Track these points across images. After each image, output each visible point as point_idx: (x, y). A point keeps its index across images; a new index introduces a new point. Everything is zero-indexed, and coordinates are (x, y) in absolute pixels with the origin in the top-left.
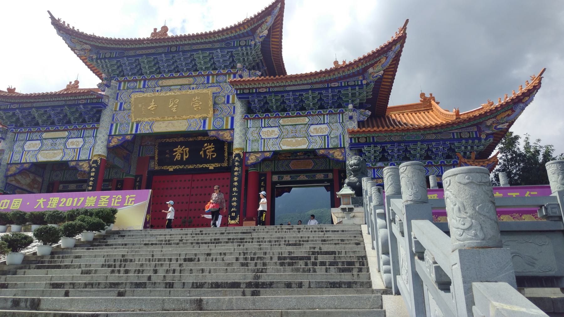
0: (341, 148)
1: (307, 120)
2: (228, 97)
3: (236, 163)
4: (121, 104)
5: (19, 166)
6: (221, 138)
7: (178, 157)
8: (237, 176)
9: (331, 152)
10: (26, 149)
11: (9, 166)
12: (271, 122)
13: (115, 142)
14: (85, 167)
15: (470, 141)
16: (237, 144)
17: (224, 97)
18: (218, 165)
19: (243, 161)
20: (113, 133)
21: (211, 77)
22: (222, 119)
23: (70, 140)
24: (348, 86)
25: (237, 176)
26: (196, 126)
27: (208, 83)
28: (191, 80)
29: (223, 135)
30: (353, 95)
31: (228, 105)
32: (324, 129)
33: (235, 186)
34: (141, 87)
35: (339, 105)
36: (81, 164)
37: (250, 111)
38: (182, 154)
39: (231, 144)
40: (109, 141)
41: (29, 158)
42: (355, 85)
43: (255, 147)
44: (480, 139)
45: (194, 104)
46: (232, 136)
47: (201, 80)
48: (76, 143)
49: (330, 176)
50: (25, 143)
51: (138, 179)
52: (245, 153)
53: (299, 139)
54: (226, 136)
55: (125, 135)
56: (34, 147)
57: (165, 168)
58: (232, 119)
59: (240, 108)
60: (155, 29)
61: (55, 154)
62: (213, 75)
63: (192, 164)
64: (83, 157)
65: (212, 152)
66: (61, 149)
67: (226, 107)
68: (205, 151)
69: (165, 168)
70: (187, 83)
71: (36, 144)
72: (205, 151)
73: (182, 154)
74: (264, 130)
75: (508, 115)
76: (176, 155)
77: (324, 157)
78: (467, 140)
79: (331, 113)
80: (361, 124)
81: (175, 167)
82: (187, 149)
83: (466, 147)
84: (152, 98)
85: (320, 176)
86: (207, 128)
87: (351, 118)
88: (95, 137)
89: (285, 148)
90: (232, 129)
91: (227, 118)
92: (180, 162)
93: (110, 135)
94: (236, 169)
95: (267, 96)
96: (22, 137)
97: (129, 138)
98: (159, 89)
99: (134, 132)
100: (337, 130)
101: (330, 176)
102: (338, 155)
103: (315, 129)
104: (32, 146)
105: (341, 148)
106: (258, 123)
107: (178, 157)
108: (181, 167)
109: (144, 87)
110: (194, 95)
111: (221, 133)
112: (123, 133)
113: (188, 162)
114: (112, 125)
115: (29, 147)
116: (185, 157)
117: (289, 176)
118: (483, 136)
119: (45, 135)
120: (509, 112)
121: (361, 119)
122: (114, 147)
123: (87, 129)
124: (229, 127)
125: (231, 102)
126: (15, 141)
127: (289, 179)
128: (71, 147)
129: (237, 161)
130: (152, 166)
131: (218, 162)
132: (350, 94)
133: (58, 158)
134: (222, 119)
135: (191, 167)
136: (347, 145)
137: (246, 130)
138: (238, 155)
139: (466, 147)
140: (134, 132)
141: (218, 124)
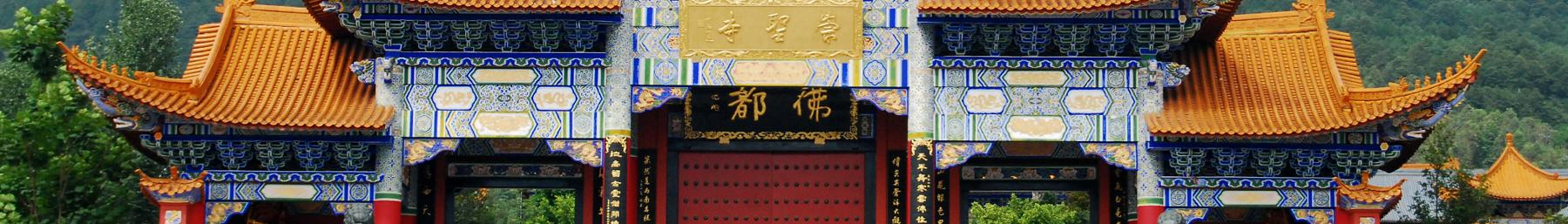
0: (1129, 142)
1: (1060, 78)
2: (893, 12)
3: (921, 167)
4: (650, 11)
5: (430, 145)
6: (881, 106)
7: (741, 112)
8: (924, 193)
9: (1110, 149)
11: (407, 143)
12: (989, 77)
13: (646, 102)
14: (588, 155)
15: (1362, 153)
17: (884, 10)
18: (835, 136)
19: (931, 160)
20: (642, 81)
23: (541, 91)
24: (1151, 20)
25: (924, 193)
29: (884, 100)
31: (894, 31)
32: (1094, 101)
33: (920, 214)
35: (1130, 52)
36: (576, 146)
37: (940, 50)
38: (750, 107)
39: (904, 119)
41: (455, 129)
42: (1162, 19)
44: (1377, 148)
46: (906, 103)
48: (555, 97)
49: (1092, 172)
51: (647, 160)
52: (935, 143)
53: (1047, 119)
54: (891, 103)
56: (457, 100)
57: (710, 135)
58: (905, 63)
59: (920, 48)
61: (512, 120)
64: (580, 132)
65: (822, 103)
66: (525, 111)
67: (886, 35)
68: (804, 102)
69: (710, 135)
71: (462, 95)
72: (804, 102)
73: (750, 107)
75: (1426, 118)
76: (735, 107)
77: (1096, 160)
78: (1357, 148)
79: (1112, 68)
80: (1170, 95)
81: (739, 135)
82: (764, 95)
83: (1355, 161)
86: (850, 84)
87: (1151, 84)
88: (600, 86)
90: (905, 87)
92: (747, 124)
93: (635, 84)
94: (921, 177)
95: (984, 26)
97: (678, 93)
101: (1092, 172)
102: (1121, 157)
103: (1078, 98)
104: (452, 98)
105: (1129, 142)
106: (958, 77)
107: (741, 112)
111: (881, 95)
112: (666, 81)
113: (767, 123)
114: (636, 62)
118: (1384, 147)
120: (1427, 113)
121: (1171, 84)
122: (647, 113)
123: (580, 67)
125: (898, 24)
126: (409, 85)
127: (1001, 177)
129: (922, 161)
131: (837, 130)
132: (1152, 37)
133: (523, 131)
135: (771, 136)
138: (923, 149)
139: (1355, 161)
140: (690, 82)
141: (875, 77)
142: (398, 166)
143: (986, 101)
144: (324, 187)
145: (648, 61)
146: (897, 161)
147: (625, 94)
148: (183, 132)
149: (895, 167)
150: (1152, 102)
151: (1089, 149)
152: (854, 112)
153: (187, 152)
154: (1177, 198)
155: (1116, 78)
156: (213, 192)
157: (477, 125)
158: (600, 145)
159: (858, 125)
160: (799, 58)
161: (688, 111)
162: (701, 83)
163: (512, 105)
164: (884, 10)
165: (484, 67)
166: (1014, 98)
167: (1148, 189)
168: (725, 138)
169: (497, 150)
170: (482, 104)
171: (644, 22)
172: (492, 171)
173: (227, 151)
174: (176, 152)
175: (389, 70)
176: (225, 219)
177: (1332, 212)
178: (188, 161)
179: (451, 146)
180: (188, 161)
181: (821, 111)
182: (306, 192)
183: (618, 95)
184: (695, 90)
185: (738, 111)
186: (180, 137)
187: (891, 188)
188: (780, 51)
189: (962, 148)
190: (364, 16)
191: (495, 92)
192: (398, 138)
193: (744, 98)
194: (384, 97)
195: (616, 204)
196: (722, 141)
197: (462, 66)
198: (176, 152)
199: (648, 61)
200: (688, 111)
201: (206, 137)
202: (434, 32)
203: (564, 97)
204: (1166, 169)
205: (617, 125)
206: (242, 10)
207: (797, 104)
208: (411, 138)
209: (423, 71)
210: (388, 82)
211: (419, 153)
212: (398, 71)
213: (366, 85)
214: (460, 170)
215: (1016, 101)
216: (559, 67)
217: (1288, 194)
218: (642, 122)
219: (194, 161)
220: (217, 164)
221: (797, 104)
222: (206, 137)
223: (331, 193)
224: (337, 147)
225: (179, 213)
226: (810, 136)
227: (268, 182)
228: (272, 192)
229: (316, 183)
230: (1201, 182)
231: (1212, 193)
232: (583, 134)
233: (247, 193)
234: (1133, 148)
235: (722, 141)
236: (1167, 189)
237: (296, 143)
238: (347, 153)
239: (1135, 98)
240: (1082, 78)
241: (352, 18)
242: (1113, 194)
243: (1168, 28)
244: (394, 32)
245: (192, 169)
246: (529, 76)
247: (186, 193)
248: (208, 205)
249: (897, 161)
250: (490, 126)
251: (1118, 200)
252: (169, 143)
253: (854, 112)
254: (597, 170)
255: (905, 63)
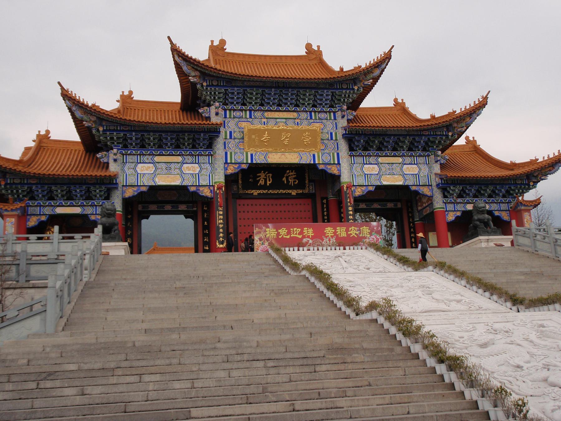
0: (429, 185)
1: (400, 160)
2: (331, 134)
4: (231, 133)
5: (135, 189)
6: (329, 171)
7: (262, 182)
9: (421, 188)
10: (139, 172)
11: (125, 188)
12: (372, 160)
13: (231, 170)
14: (206, 192)
16: (345, 178)
17: (328, 133)
20: (229, 161)
21: (313, 113)
22: (329, 154)
23: (185, 165)
24: (436, 135)
26: (306, 159)
27: (311, 118)
28: (295, 114)
29: (330, 169)
30: (440, 142)
31: (332, 141)
33: (350, 215)
34: (248, 117)
36: (201, 189)
39: (339, 176)
40: (226, 169)
43: (360, 181)
45: (304, 139)
47: (304, 115)
49: (399, 205)
50: (136, 166)
53: (396, 176)
54: (334, 170)
55: (240, 164)
56: (147, 170)
58: (338, 154)
59: (343, 146)
60: (212, 42)
62: (315, 112)
63: (273, 189)
64: (202, 183)
65: (294, 178)
67: (331, 144)
68: (287, 178)
69: (249, 192)
70: (292, 117)
72: (287, 178)
74: (365, 166)
76: (259, 180)
81: (261, 191)
82: (271, 175)
84: (266, 130)
85: (390, 205)
89: (385, 183)
90: (339, 164)
91: (333, 154)
93: (226, 163)
96: (130, 158)
98: (265, 120)
99: (249, 162)
100: (425, 170)
102: (426, 191)
103: (408, 168)
105: (429, 185)
106: (359, 160)
107: (262, 182)
108: (264, 192)
109: (251, 117)
110: (305, 131)
111: (329, 167)
113: (271, 187)
114: (226, 153)
115: (142, 170)
116: (268, 183)
117: (364, 204)
119: (157, 159)
120: (551, 168)
122: (232, 175)
124: (336, 163)
125: (334, 138)
126: (124, 163)
127: (365, 207)
128: (187, 172)
130: (235, 189)
131: (301, 189)
134: (329, 154)
136: (434, 184)
137: (352, 164)
140: (249, 162)
141: (327, 159)
142: (121, 199)
143: (371, 169)
144: (85, 208)
145: (231, 153)
146: (325, 201)
147: (222, 166)
148: (16, 182)
149: (324, 204)
150: (437, 169)
151: (413, 188)
152: (307, 182)
153: (17, 191)
154: (450, 207)
155: (421, 160)
156: (30, 210)
157: (157, 180)
158: (212, 188)
159: (308, 187)
160: (295, 152)
161: (240, 182)
162: (254, 162)
163: (173, 171)
164: (328, 133)
165: (159, 155)
166: (382, 168)
167: (439, 203)
168: (255, 192)
169: (160, 199)
170: (159, 171)
171: (228, 137)
172: (157, 208)
173: (39, 191)
174: (12, 191)
175: (115, 154)
176: (37, 223)
177: (508, 212)
178: (18, 196)
179: (144, 189)
180: (18, 196)
181: (294, 182)
182: (77, 210)
183: (219, 167)
184: (252, 164)
185: (261, 182)
186: (14, 183)
187: (323, 212)
188: (288, 148)
189: (364, 188)
190: (104, 130)
191: (164, 166)
192: (120, 185)
193: (262, 175)
194: (113, 168)
195: (221, 213)
196: (254, 194)
197: (149, 155)
198: (12, 191)
199: (231, 153)
200: (240, 182)
201: (27, 184)
202: (136, 139)
203: (195, 168)
204: (445, 197)
205: (220, 178)
206: (44, 141)
207: (284, 179)
208: (126, 186)
209: (131, 157)
210: (115, 160)
211: (130, 193)
212: (119, 156)
213: (104, 163)
214: (143, 207)
215: (383, 169)
216: (192, 155)
217: (492, 205)
218: (230, 179)
219: (21, 196)
220: (32, 198)
221: (284, 179)
222: (27, 184)
223: (89, 211)
224: (92, 188)
225: (13, 220)
226: (290, 191)
227: (58, 206)
228: (60, 210)
229: (82, 206)
230: (459, 200)
231: (463, 205)
232: (204, 183)
233: (48, 211)
234: (430, 188)
235: (254, 194)
236: (445, 203)
237: (72, 187)
238: (97, 191)
239: (430, 168)
240: (408, 160)
241: (98, 131)
242: (408, 213)
243: (444, 138)
244: (118, 138)
245: (21, 200)
246: (180, 159)
247: (17, 209)
248: (28, 217)
249: (325, 201)
250: (161, 181)
251: (410, 215)
252: (8, 186)
253: (307, 182)
254: (212, 198)
255: (338, 154)
